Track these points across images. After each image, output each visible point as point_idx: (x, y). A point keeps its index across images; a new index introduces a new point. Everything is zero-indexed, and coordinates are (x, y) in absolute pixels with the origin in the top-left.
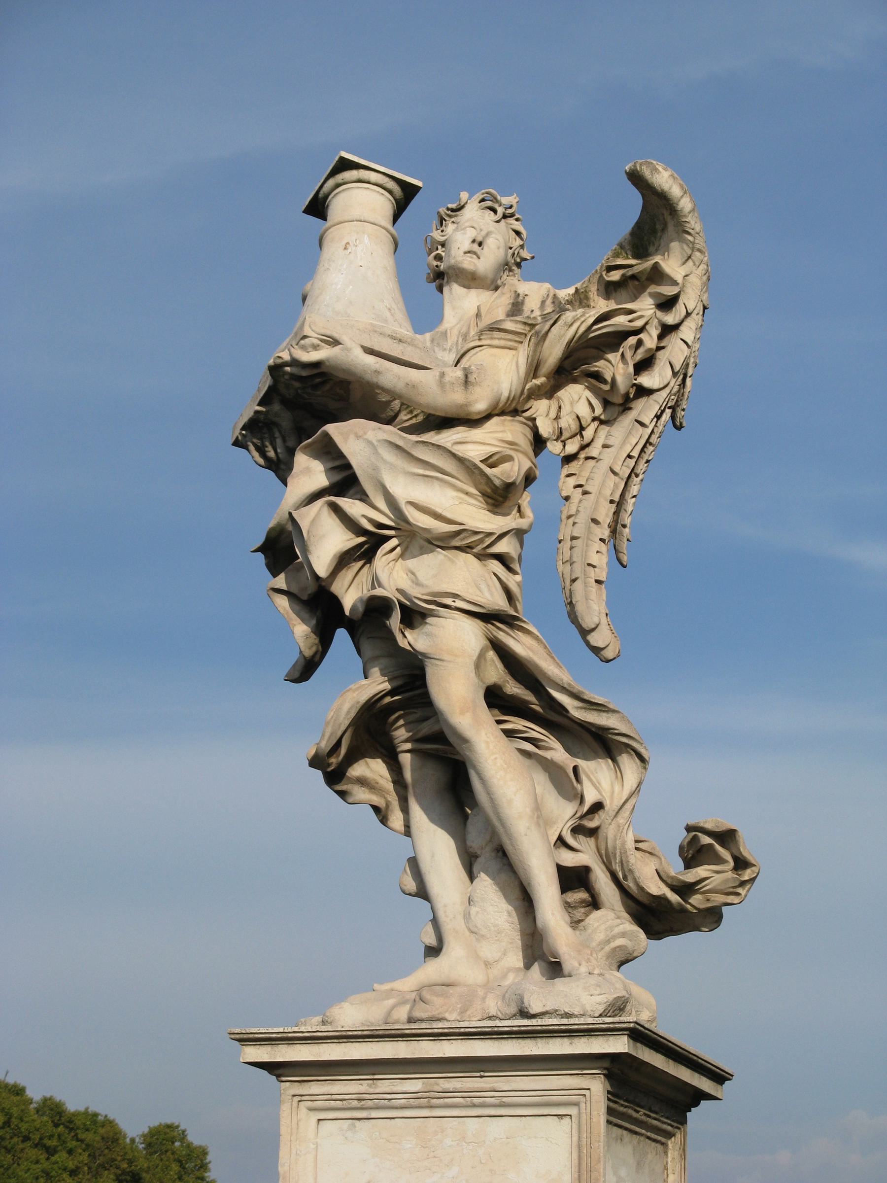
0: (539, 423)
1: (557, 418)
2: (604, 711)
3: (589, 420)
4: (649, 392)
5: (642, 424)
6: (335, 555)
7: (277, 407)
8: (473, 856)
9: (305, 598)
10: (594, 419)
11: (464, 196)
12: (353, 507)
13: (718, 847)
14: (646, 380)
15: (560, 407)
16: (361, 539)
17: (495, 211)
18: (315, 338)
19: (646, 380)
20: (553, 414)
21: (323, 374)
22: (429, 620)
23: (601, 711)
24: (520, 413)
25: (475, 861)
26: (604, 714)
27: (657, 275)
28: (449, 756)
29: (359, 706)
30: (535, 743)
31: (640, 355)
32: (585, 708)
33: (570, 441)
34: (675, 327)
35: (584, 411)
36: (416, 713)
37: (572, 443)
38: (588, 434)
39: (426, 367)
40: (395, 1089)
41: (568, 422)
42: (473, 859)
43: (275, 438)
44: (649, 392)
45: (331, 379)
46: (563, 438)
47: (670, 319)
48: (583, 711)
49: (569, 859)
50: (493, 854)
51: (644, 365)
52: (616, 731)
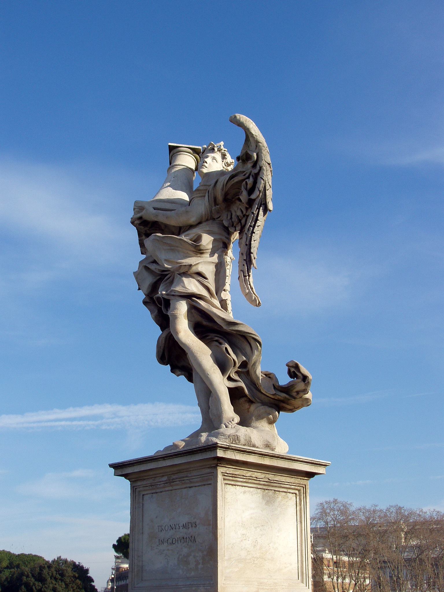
0: (224, 222)
1: (231, 218)
3: (242, 216)
6: (149, 285)
10: (244, 216)
14: (253, 197)
15: (232, 214)
16: (158, 278)
18: (137, 208)
19: (253, 197)
20: (229, 217)
24: (216, 219)
33: (237, 226)
35: (239, 213)
38: (243, 221)
39: (172, 210)
40: (161, 480)
41: (235, 219)
46: (234, 225)
51: (251, 191)
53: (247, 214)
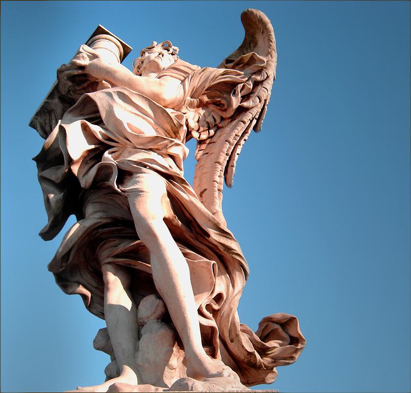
2: (229, 238)
4: (246, 110)
5: (244, 123)
7: (56, 100)
8: (141, 326)
9: (58, 181)
10: (216, 125)
11: (155, 43)
12: (96, 129)
13: (280, 330)
17: (168, 51)
21: (85, 75)
22: (135, 176)
23: (228, 237)
25: (141, 329)
26: (229, 240)
27: (253, 60)
28: (132, 267)
29: (84, 229)
30: (187, 256)
31: (244, 92)
32: (219, 234)
34: (261, 82)
36: (115, 241)
37: (204, 134)
42: (140, 327)
43: (52, 120)
44: (246, 110)
45: (88, 80)
46: (200, 131)
47: (259, 78)
48: (219, 236)
49: (205, 322)
50: (156, 321)
52: (235, 252)
53: (220, 125)
